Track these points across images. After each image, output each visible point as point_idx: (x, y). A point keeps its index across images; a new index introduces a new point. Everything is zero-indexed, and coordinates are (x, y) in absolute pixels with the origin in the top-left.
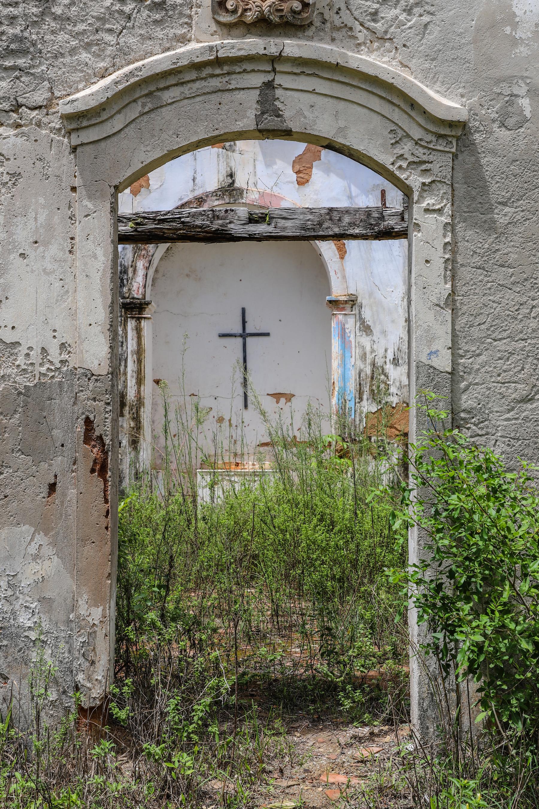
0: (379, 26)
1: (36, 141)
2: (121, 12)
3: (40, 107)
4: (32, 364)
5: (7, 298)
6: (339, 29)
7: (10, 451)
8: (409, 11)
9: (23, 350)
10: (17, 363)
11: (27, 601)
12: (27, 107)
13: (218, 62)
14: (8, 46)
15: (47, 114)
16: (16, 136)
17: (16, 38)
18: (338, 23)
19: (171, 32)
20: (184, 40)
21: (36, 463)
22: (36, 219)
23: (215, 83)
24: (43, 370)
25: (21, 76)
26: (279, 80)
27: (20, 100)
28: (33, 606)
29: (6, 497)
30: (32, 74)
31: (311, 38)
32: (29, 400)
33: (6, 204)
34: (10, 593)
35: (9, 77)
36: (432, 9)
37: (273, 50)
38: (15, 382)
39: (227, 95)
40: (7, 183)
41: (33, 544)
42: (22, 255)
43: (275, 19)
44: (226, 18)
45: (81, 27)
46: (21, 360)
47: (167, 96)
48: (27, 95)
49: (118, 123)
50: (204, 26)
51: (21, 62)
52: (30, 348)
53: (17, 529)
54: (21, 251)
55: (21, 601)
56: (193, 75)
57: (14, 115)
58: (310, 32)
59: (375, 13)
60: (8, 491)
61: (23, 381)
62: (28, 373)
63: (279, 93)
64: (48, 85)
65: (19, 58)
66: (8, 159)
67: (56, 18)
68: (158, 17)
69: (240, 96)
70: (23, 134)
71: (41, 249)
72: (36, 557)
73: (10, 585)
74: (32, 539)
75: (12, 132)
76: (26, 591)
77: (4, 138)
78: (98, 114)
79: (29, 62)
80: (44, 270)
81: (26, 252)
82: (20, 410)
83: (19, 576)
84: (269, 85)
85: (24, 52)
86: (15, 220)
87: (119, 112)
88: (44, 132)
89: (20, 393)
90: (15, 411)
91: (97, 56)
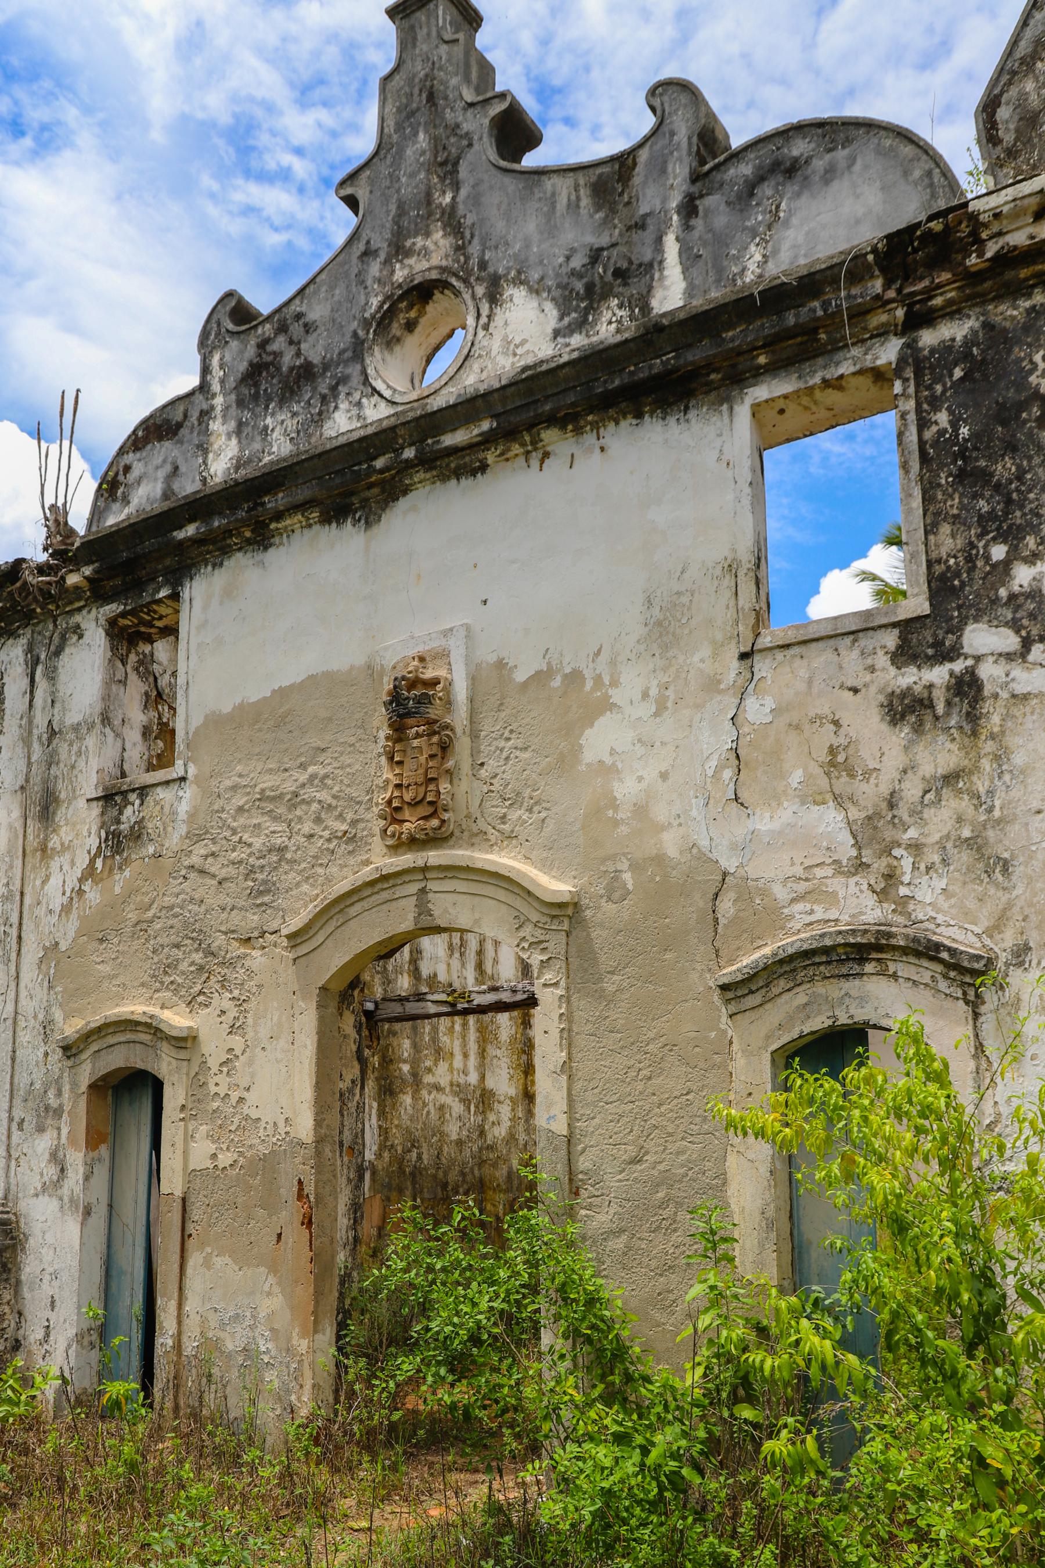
0: (506, 827)
2: (328, 849)
6: (477, 835)
8: (530, 810)
13: (384, 878)
17: (265, 882)
18: (475, 830)
19: (359, 858)
20: (367, 863)
23: (385, 895)
26: (431, 885)
31: (452, 847)
36: (548, 805)
37: (420, 863)
39: (394, 903)
43: (420, 836)
44: (390, 842)
45: (303, 865)
47: (353, 911)
49: (320, 938)
50: (378, 850)
51: (266, 899)
56: (368, 891)
58: (451, 842)
59: (504, 816)
63: (431, 896)
67: (288, 862)
68: (351, 848)
69: (403, 903)
78: (307, 932)
84: (423, 891)
85: (268, 891)
87: (321, 928)
91: (312, 885)
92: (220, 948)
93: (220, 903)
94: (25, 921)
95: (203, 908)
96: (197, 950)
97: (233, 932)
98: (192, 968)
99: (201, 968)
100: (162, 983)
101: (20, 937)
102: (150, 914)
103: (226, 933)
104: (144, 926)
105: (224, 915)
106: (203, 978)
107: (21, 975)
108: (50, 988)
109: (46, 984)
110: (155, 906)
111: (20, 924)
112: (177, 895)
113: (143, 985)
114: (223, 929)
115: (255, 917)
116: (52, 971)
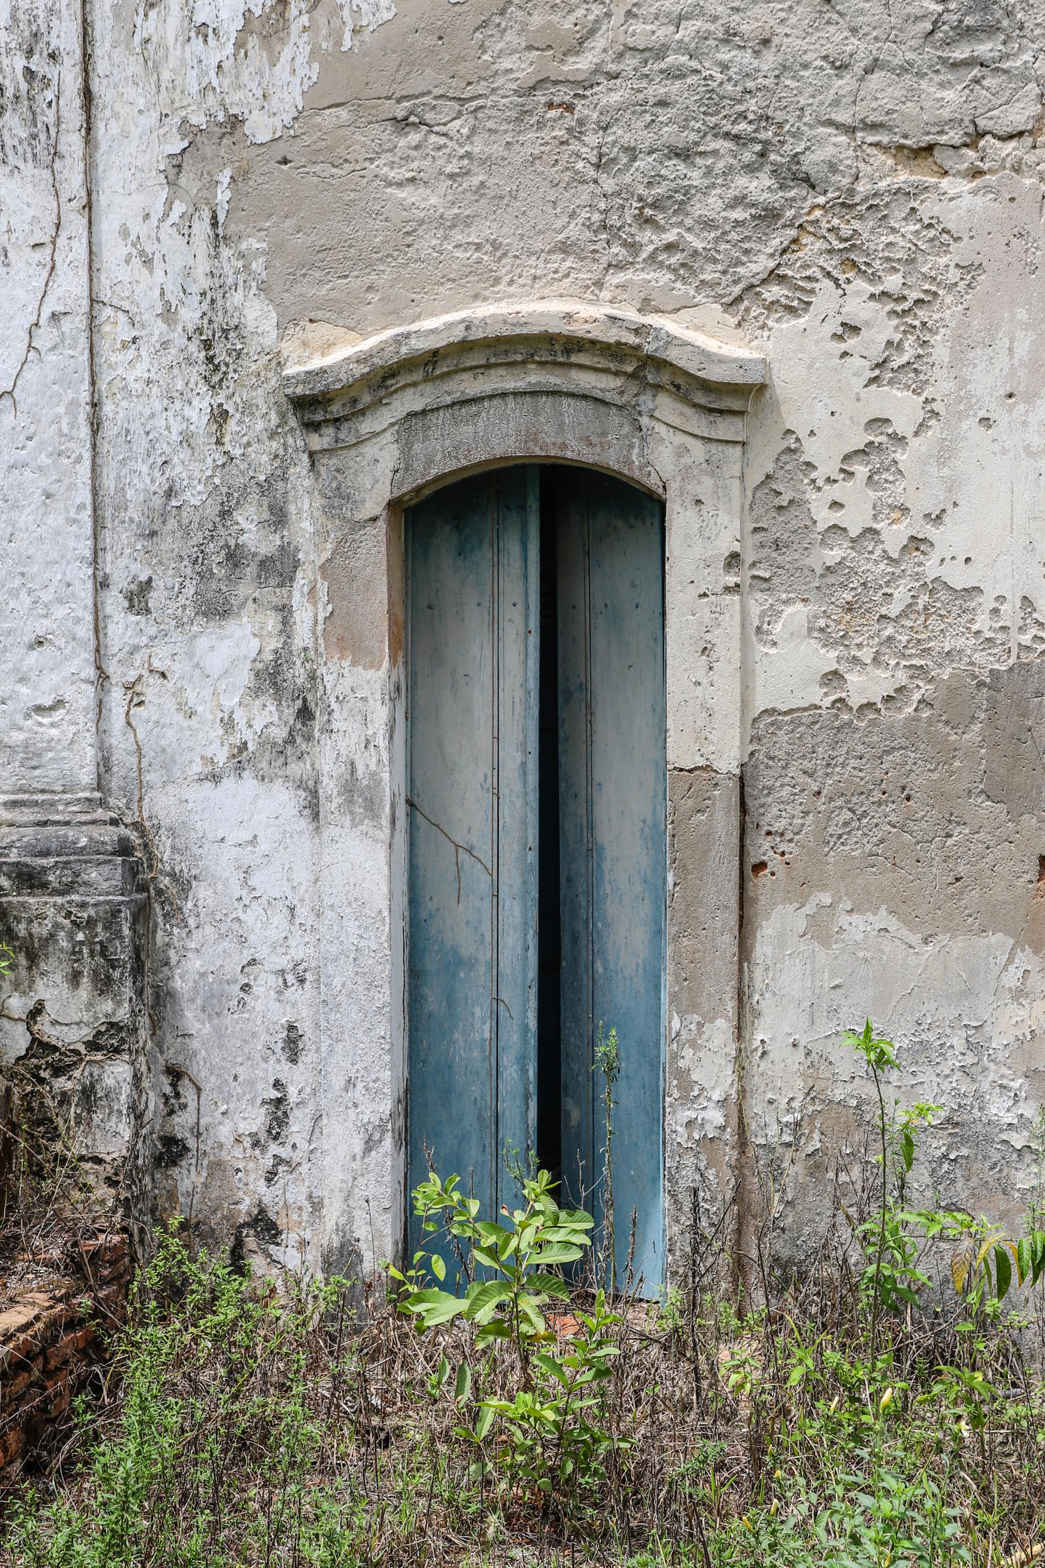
1: (1012, 200)
3: (1021, 134)
4: (1004, 628)
5: (955, 504)
7: (965, 794)
9: (987, 602)
10: (975, 627)
11: (1002, 1076)
12: (994, 136)
14: (960, 21)
15: (1034, 147)
16: (974, 192)
21: (1014, 816)
22: (1011, 350)
24: (1026, 639)
25: (983, 77)
27: (983, 123)
28: (1015, 1085)
29: (957, 880)
30: (1005, 72)
32: (1000, 697)
33: (953, 324)
34: (970, 1059)
35: (960, 80)
38: (972, 664)
40: (956, 284)
41: (1011, 968)
42: (985, 421)
46: (982, 622)
48: (995, 112)
51: (984, 49)
52: (1001, 599)
53: (982, 941)
54: (982, 414)
55: (992, 1076)
57: (970, 153)
60: (962, 870)
61: (987, 662)
62: (996, 646)
64: (1037, 91)
65: (981, 41)
66: (958, 239)
70: (987, 189)
71: (1022, 407)
72: (1018, 994)
73: (970, 1045)
74: (1010, 960)
75: (965, 186)
76: (1001, 1056)
77: (951, 199)
79: (1000, 47)
80: (1027, 449)
81: (993, 416)
82: (983, 716)
83: (987, 1028)
85: (991, 30)
86: (971, 356)
88: (1027, 182)
89: (981, 684)
90: (973, 717)
92: (833, 168)
93: (830, 49)
94: (101, 51)
95: (769, 60)
96: (750, 169)
97: (875, 127)
98: (738, 214)
99: (769, 216)
100: (633, 247)
101: (87, 95)
102: (582, 64)
103: (850, 130)
104: (564, 94)
105: (845, 83)
106: (777, 241)
107: (103, 199)
108: (218, 239)
109: (202, 228)
110: (599, 42)
111: (87, 58)
112: (678, 20)
113: (564, 248)
114: (843, 116)
115: (949, 95)
116: (223, 195)
